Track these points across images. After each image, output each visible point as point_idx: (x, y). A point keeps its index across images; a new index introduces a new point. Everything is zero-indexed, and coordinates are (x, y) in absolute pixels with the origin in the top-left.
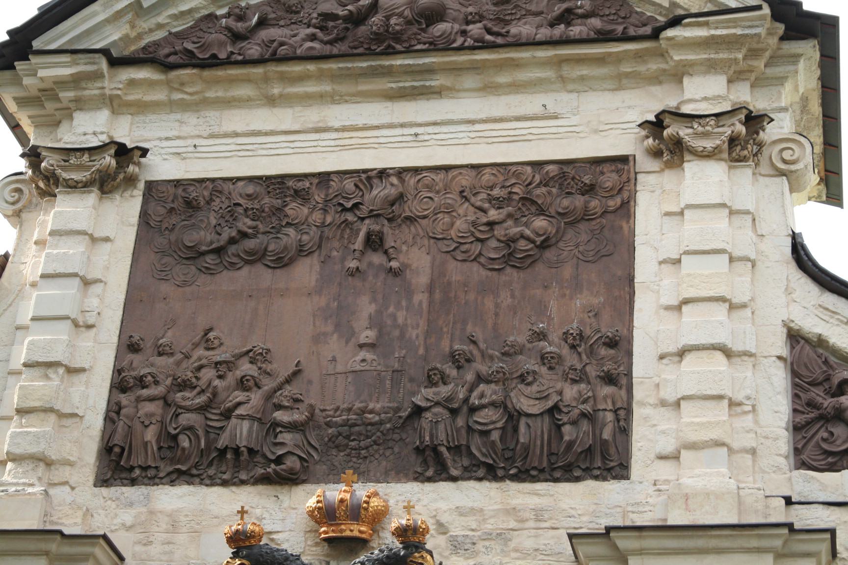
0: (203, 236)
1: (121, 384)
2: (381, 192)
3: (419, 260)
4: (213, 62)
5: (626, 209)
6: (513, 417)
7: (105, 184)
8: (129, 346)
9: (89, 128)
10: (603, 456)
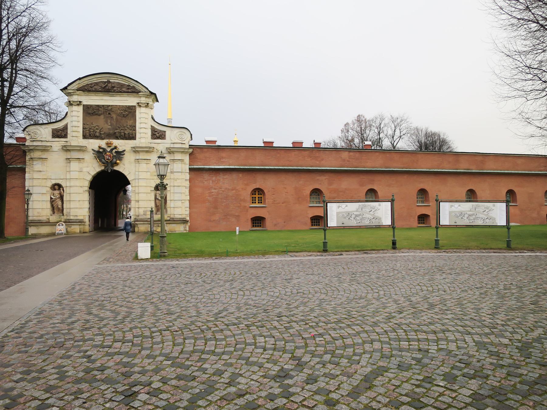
0: (90, 112)
1: (83, 128)
2: (110, 108)
3: (114, 116)
4: (89, 91)
5: (135, 112)
6: (125, 134)
7: (78, 105)
8: (84, 124)
9: (75, 98)
10: (134, 138)
